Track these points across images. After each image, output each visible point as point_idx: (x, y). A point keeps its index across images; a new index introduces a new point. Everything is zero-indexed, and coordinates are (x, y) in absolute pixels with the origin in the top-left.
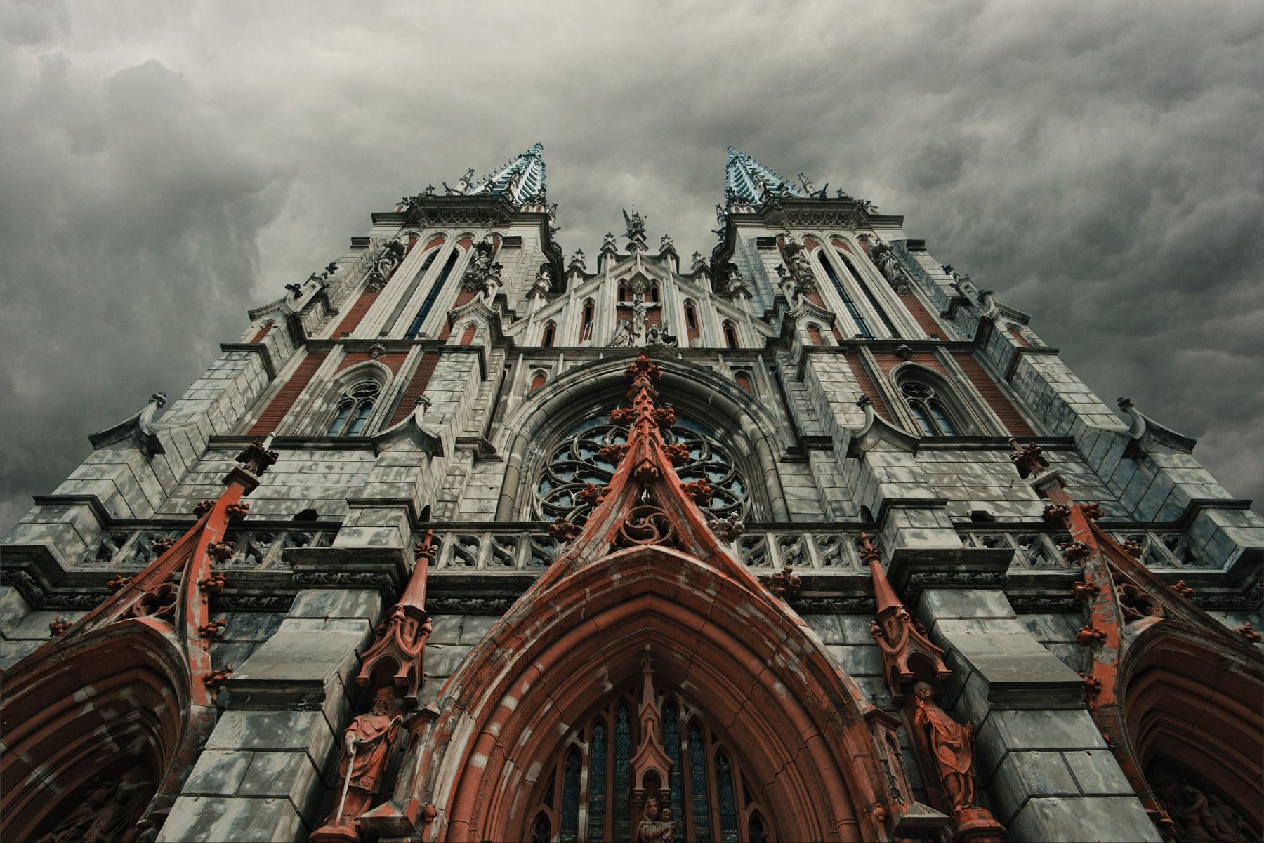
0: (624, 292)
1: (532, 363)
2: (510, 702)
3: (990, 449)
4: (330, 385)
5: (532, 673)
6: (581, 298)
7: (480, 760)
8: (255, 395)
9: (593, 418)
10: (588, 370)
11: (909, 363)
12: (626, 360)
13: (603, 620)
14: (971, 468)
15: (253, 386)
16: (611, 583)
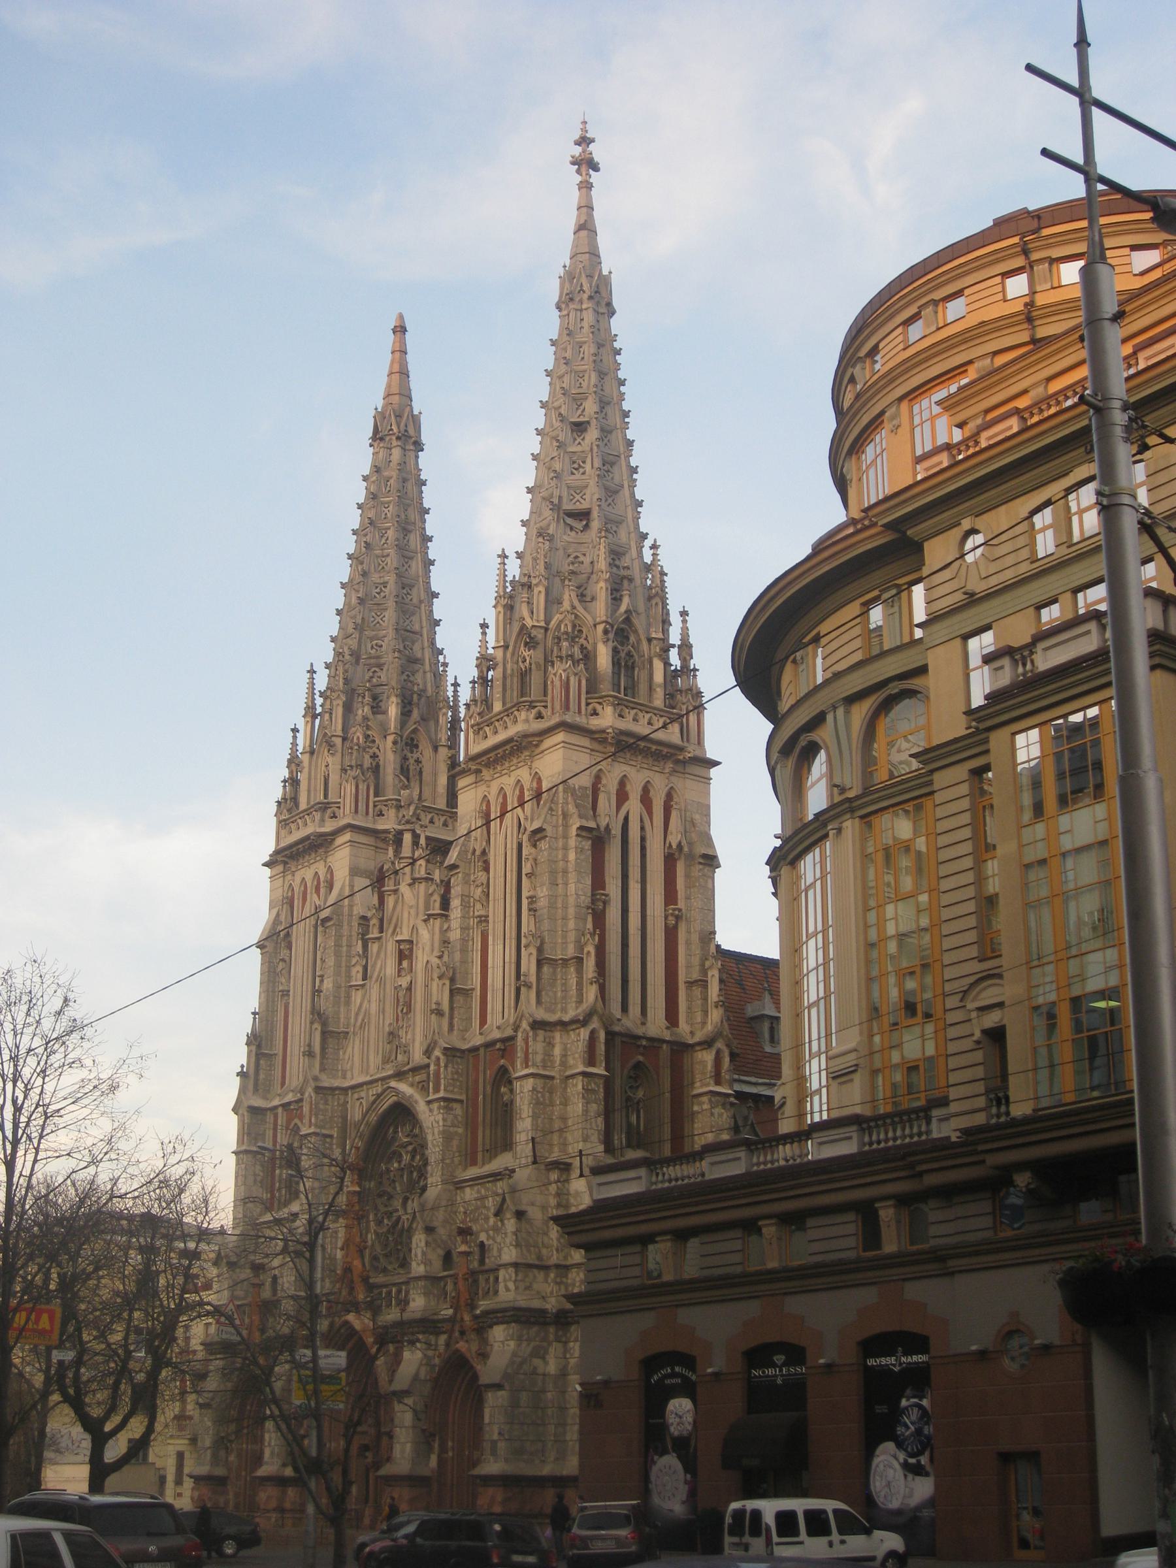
1: (356, 1096)
6: (377, 980)
8: (261, 1174)
11: (502, 1062)
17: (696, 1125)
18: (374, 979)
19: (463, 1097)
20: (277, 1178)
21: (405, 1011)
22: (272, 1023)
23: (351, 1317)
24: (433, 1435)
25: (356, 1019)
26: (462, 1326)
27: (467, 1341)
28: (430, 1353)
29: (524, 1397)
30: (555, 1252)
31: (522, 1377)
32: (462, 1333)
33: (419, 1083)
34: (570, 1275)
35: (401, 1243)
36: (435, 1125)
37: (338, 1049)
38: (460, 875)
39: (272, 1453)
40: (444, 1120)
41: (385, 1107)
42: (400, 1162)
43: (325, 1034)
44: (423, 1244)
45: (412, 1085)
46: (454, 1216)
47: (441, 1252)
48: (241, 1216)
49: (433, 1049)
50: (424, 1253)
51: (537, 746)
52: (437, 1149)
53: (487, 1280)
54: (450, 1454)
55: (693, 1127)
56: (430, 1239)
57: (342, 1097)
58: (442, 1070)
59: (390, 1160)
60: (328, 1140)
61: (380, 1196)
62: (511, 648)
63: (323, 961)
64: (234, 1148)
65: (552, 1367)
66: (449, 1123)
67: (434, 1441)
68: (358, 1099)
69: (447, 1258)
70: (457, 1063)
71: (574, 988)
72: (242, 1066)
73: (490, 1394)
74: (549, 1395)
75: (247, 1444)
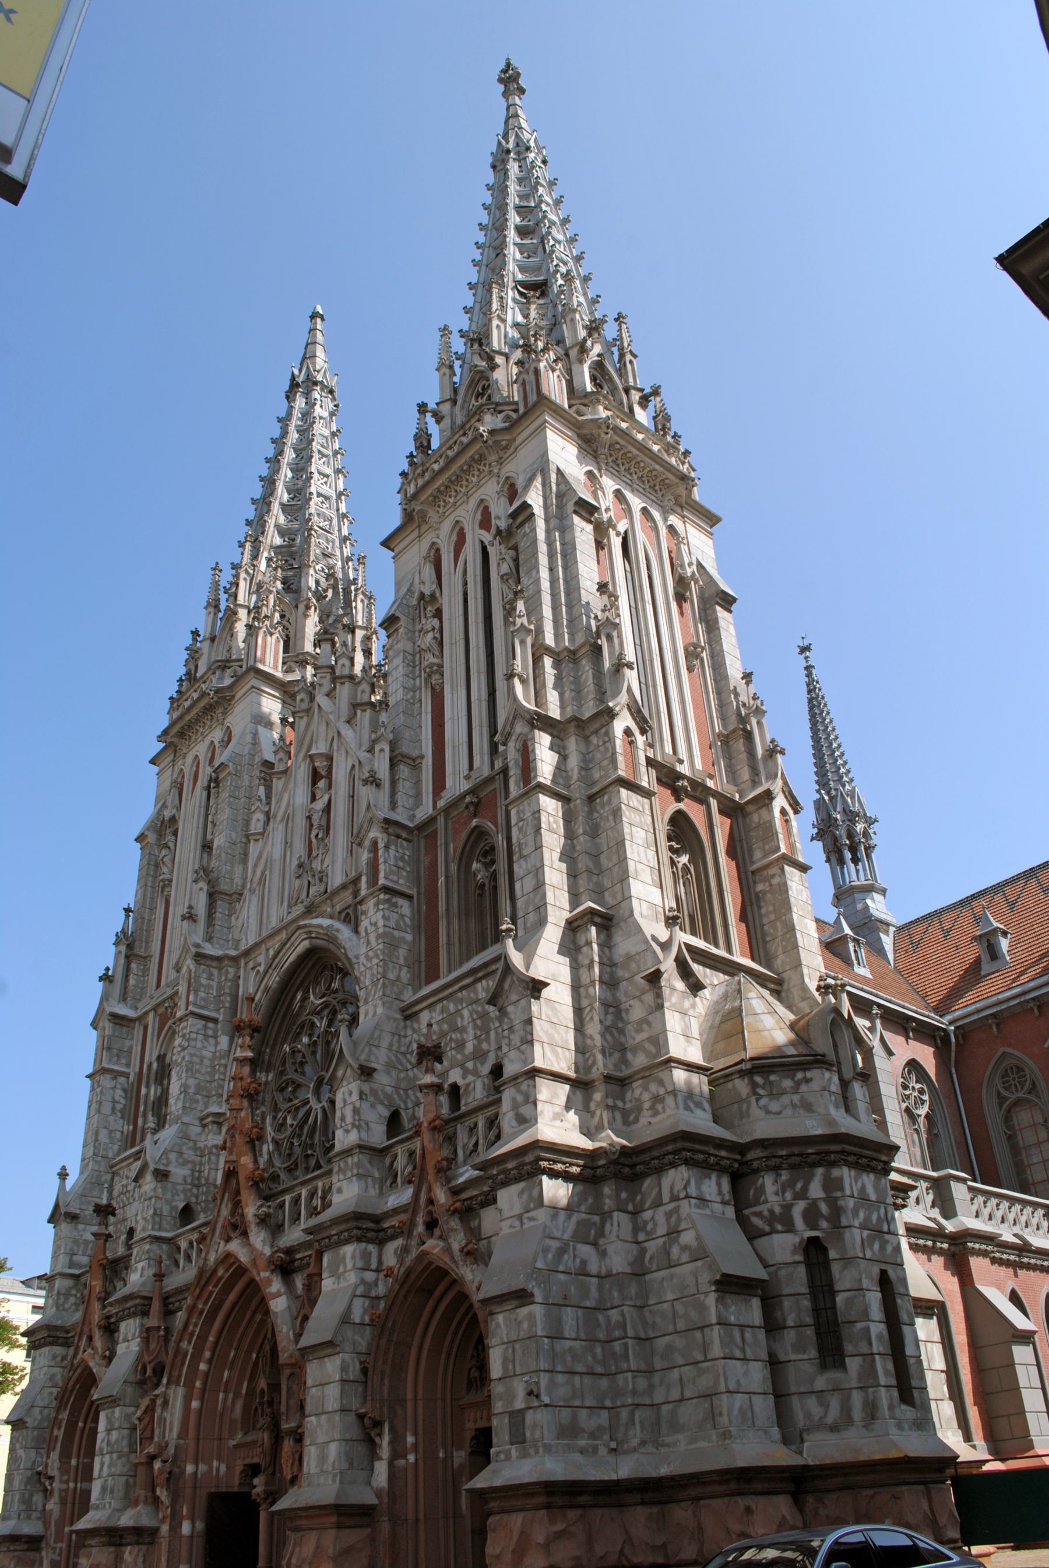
0: (315, 776)
1: (251, 965)
2: (203, 1366)
3: (479, 980)
4: (155, 1066)
5: (209, 1345)
6: (282, 820)
7: (195, 1404)
8: (123, 1101)
9: (301, 1006)
10: (270, 971)
11: (474, 822)
12: (292, 940)
13: (232, 1297)
14: (462, 1018)
15: (117, 1098)
16: (221, 1278)
17: (763, 911)
18: (279, 818)
19: (413, 892)
20: (142, 1101)
21: (320, 836)
22: (150, 920)
23: (235, 1246)
24: (378, 1424)
25: (254, 872)
26: (430, 1213)
27: (441, 1237)
28: (369, 1276)
29: (570, 1317)
30: (599, 1057)
31: (562, 1276)
32: (431, 1225)
33: (340, 913)
34: (628, 1096)
35: (312, 1146)
36: (371, 929)
37: (230, 916)
38: (401, 630)
39: (104, 1489)
40: (384, 917)
41: (292, 959)
42: (310, 1036)
43: (212, 896)
44: (355, 1097)
45: (331, 917)
46: (400, 1057)
47: (386, 1113)
48: (91, 1153)
49: (368, 831)
50: (356, 1111)
51: (506, 448)
52: (375, 961)
53: (473, 1129)
54: (411, 1458)
55: (760, 915)
56: (366, 1088)
57: (231, 971)
58: (380, 852)
59: (297, 1036)
60: (211, 1025)
61: (282, 1090)
62: (459, 403)
63: (214, 824)
64: (90, 1070)
65: (618, 1260)
66: (392, 924)
67: (380, 1435)
68: (253, 969)
69: (394, 1122)
70: (402, 846)
71: (590, 681)
72: (107, 969)
73: (500, 1318)
74: (614, 1315)
75: (76, 1482)
